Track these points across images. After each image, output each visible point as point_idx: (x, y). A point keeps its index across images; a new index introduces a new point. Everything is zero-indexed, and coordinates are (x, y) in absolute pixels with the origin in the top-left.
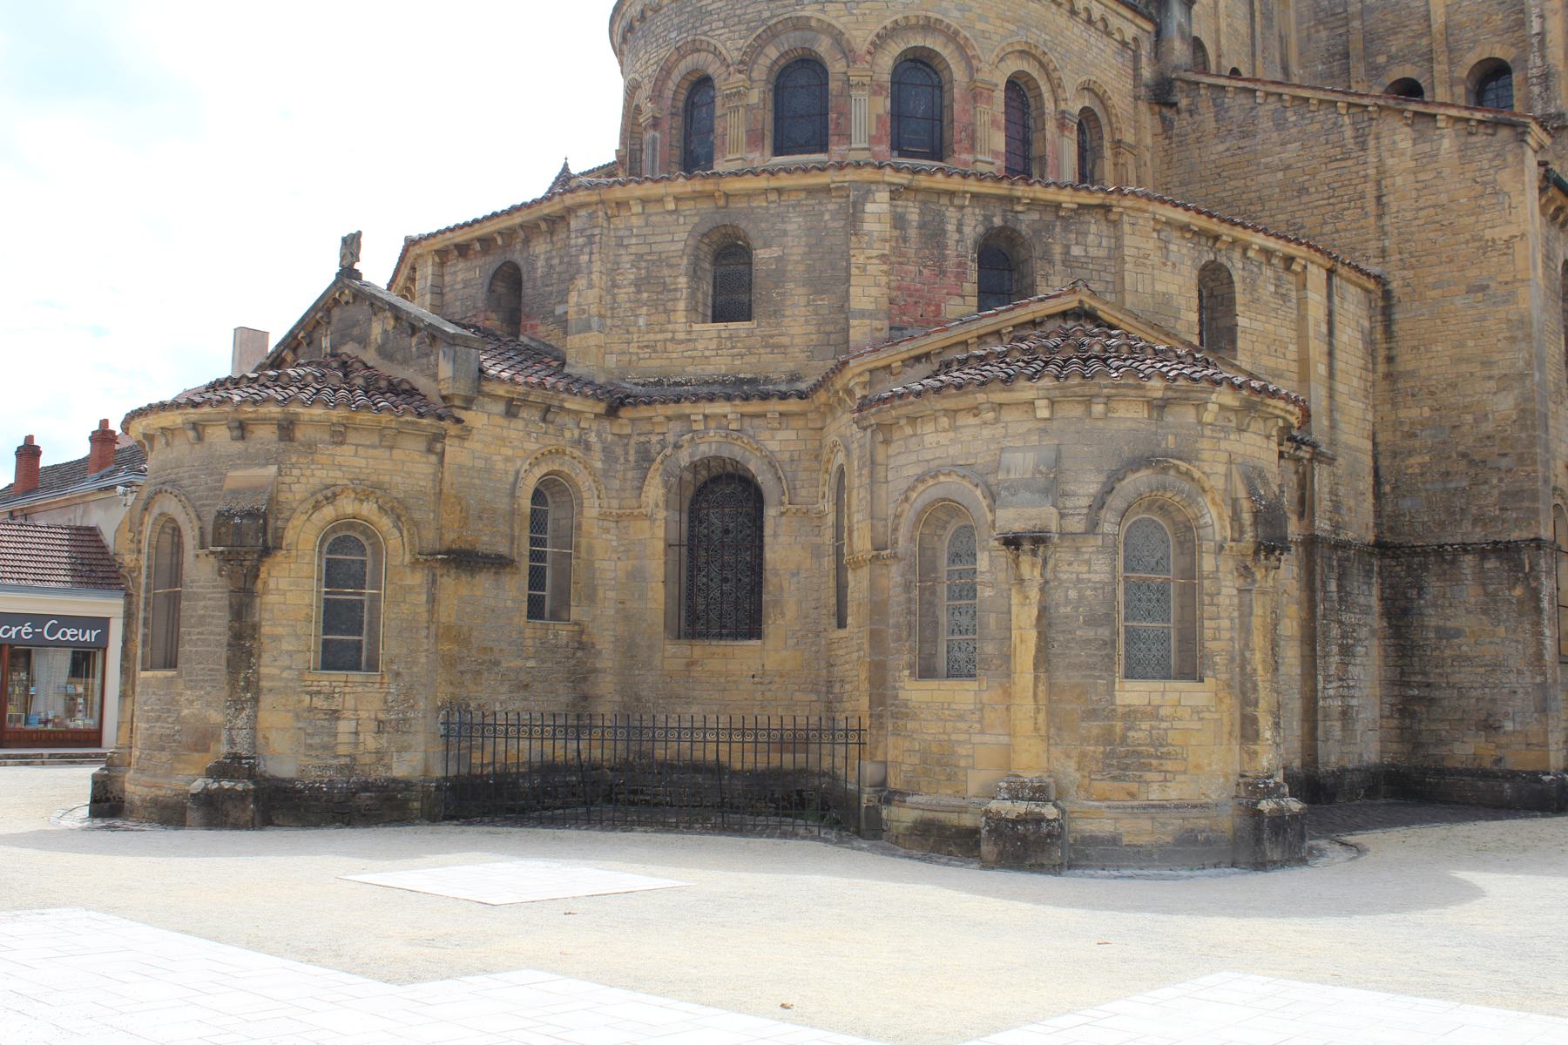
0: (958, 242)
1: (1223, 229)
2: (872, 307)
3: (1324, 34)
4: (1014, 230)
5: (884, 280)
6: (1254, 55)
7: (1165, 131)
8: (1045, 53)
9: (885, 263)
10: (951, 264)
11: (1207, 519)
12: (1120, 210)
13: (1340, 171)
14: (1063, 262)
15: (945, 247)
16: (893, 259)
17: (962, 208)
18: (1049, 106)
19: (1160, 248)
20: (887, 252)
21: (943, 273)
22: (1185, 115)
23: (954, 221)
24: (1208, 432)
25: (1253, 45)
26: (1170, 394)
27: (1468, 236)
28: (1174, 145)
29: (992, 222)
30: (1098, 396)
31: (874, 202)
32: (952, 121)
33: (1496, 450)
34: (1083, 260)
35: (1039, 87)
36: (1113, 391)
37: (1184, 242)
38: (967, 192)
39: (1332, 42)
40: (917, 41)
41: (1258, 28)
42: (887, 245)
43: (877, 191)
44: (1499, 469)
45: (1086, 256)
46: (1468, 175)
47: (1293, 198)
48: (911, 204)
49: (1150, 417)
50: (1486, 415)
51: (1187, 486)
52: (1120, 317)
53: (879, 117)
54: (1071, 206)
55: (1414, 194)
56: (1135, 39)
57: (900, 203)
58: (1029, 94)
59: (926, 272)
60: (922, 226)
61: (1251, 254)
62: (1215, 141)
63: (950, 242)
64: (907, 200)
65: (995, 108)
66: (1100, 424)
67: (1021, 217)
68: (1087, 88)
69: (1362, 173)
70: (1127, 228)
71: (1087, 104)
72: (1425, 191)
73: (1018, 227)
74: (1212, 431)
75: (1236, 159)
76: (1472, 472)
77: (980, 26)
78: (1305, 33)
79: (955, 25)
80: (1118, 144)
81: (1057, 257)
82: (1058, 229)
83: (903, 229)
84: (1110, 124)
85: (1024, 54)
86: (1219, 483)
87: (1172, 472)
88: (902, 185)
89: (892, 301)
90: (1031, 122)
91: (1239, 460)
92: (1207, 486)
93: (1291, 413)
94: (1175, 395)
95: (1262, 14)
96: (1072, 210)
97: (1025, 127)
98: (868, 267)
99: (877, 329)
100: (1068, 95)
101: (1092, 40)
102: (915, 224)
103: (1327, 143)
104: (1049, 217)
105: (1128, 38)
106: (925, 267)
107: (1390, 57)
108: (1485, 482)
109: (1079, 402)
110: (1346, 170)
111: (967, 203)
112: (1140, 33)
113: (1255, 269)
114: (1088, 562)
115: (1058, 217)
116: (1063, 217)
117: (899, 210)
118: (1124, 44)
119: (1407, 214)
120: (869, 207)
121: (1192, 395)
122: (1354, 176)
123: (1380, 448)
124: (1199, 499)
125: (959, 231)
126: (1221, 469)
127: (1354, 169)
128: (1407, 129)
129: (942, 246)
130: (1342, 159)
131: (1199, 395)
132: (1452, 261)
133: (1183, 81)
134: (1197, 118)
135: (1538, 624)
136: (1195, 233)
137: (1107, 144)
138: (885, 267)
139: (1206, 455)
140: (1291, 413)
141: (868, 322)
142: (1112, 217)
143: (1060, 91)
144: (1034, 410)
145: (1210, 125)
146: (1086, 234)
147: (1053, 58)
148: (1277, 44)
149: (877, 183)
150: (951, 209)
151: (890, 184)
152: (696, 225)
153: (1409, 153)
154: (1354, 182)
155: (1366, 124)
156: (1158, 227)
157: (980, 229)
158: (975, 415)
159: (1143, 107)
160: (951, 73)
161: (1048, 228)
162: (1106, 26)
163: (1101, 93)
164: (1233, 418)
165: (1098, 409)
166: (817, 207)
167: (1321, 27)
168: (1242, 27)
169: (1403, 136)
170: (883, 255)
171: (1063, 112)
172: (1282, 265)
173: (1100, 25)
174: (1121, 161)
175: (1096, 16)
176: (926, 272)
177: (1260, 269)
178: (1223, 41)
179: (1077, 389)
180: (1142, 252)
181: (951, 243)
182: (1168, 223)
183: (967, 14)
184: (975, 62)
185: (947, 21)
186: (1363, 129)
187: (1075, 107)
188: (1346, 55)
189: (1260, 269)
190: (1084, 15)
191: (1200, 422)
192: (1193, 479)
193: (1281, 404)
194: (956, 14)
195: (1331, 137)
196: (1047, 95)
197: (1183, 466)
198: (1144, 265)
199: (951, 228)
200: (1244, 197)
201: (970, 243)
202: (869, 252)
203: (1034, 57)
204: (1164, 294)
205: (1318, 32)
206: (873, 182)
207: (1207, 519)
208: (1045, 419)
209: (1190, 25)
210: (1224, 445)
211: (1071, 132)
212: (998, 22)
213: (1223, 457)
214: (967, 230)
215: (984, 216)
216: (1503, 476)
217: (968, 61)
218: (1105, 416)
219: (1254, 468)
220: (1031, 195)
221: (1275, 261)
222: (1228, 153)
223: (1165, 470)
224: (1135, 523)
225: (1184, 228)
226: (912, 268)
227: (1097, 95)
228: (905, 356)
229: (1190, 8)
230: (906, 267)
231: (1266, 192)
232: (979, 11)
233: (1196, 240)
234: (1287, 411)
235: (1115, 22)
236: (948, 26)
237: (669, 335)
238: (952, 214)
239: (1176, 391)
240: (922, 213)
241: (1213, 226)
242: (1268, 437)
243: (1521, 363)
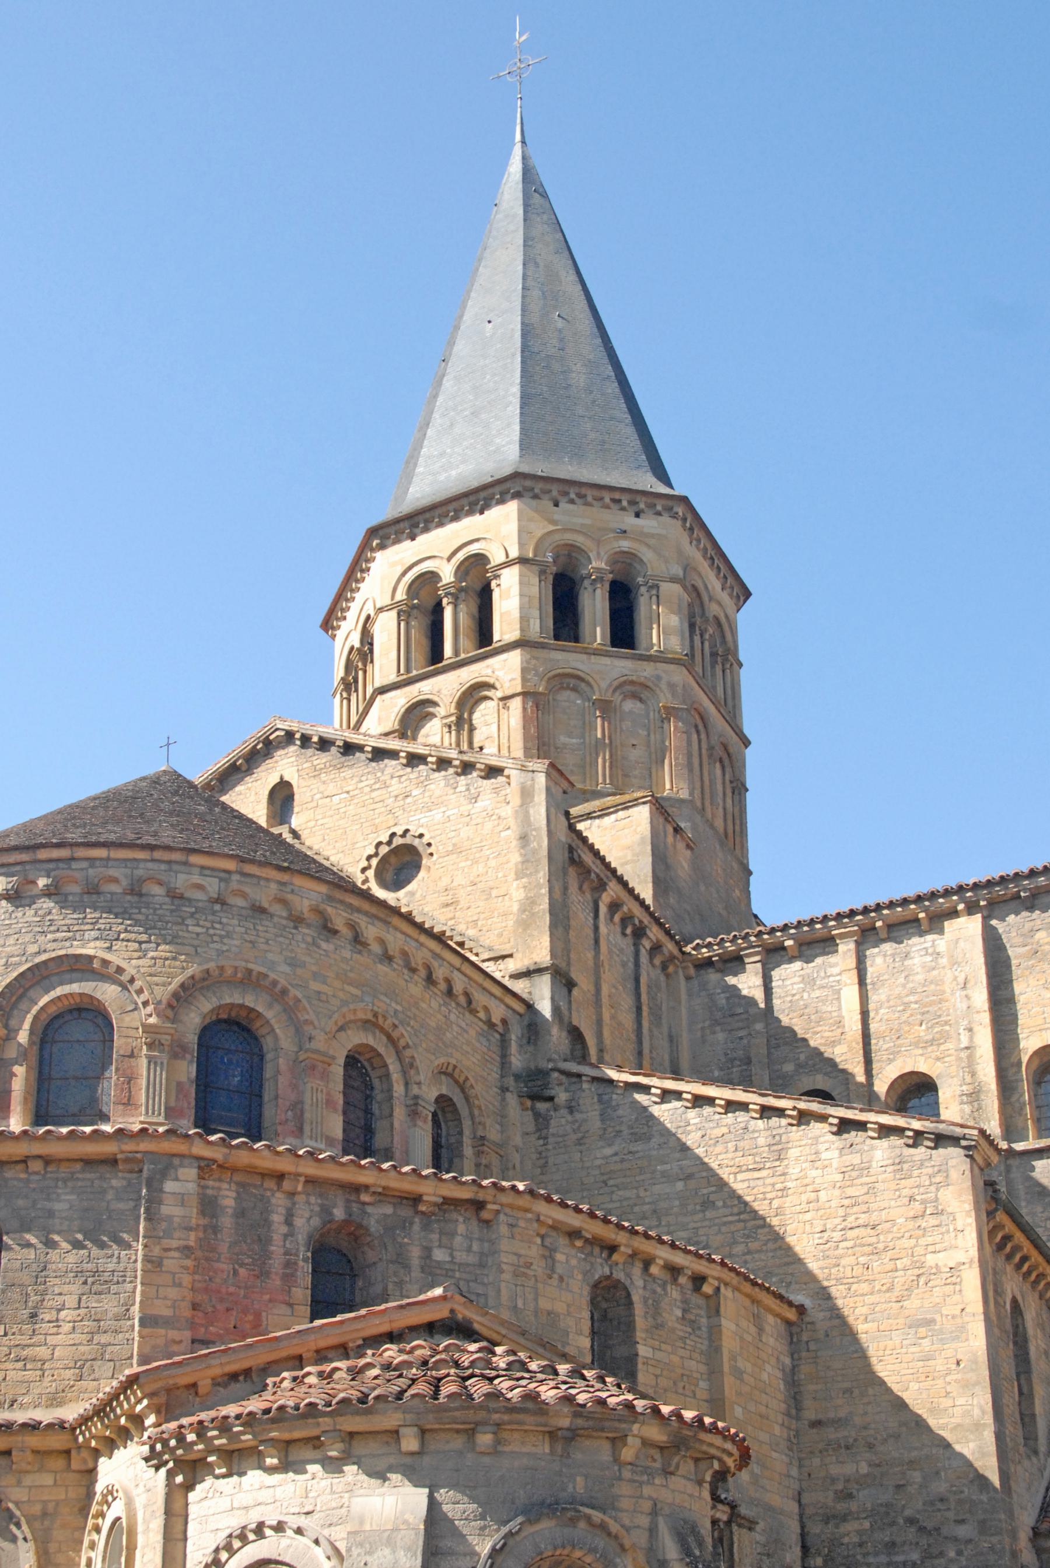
0: (286, 1236)
1: (622, 1238)
2: (167, 1312)
3: (721, 1036)
4: (360, 1226)
5: (186, 1279)
7: (538, 1130)
8: (395, 1026)
9: (188, 1257)
10: (276, 1263)
12: (496, 1207)
13: (752, 1183)
14: (422, 1268)
15: (269, 1241)
16: (199, 1253)
17: (292, 1194)
18: (399, 1089)
19: (544, 1257)
20: (192, 1244)
21: (263, 1274)
22: (564, 1112)
24: (627, 1474)
25: (640, 1042)
26: (580, 1422)
27: (906, 1261)
28: (550, 1147)
29: (331, 1214)
30: (484, 1423)
31: (177, 1179)
32: (277, 1097)
33: (951, 1515)
34: (447, 1266)
35: (385, 1066)
36: (506, 1417)
37: (573, 1252)
38: (300, 1175)
39: (731, 1046)
41: (645, 1024)
42: (193, 1235)
43: (181, 1166)
44: (956, 1539)
47: (694, 1213)
48: (225, 1186)
49: (552, 1452)
50: (937, 1473)
51: (600, 1542)
52: (504, 1332)
53: (179, 1084)
55: (841, 1212)
56: (504, 1022)
57: (211, 1183)
58: (373, 1074)
59: (242, 1271)
60: (240, 1213)
62: (601, 1143)
63: (275, 1237)
64: (220, 1180)
65: (331, 1085)
66: (486, 1460)
67: (369, 1209)
68: (446, 1072)
69: (779, 1186)
70: (504, 1230)
71: (444, 1092)
72: (855, 1209)
73: (365, 1223)
74: (633, 1472)
75: (626, 1165)
76: (924, 1542)
77: (315, 986)
78: (699, 1034)
79: (283, 982)
80: (481, 1141)
81: (415, 1262)
82: (416, 1227)
83: (214, 1216)
84: (472, 1116)
85: (371, 1024)
86: (641, 1538)
87: (582, 1524)
88: (214, 1161)
89: (195, 1307)
90: (375, 1108)
91: (667, 1510)
92: (627, 1543)
93: (730, 1454)
94: (586, 1424)
95: (650, 1008)
96: (435, 1204)
97: (368, 1111)
98: (166, 1262)
99: (174, 1342)
100: (422, 1078)
101: (453, 1017)
102: (230, 1211)
103: (736, 1150)
104: (406, 1212)
105: (496, 1019)
106: (242, 1265)
107: (799, 1066)
108: (941, 1554)
109: (458, 1431)
110: (760, 1182)
111: (300, 1188)
112: (509, 1014)
113: (659, 1290)
115: (417, 1212)
116: (423, 1213)
117: (209, 1192)
118: (491, 1025)
119: (835, 1234)
120: (169, 1186)
121: (607, 1424)
122: (769, 1189)
124: (618, 1560)
125: (289, 1221)
126: (644, 1521)
127: (769, 1181)
129: (264, 1241)
130: (754, 1170)
131: (617, 1424)
132: (888, 1290)
133: (563, 1072)
134: (578, 1116)
136: (587, 1240)
137: (467, 1140)
138: (189, 1263)
139: (625, 1503)
140: (730, 1454)
141: (162, 1331)
142: (485, 1215)
143: (412, 1072)
144: (398, 1440)
145: (595, 1124)
146: (453, 1234)
147: (406, 1036)
148: (665, 1044)
149: (182, 1156)
150: (278, 1195)
151: (199, 1158)
153: (835, 1164)
154: (769, 1196)
155: (782, 1131)
156: (543, 1231)
157: (316, 1222)
158: (315, 1448)
160: (276, 1038)
161: (405, 1225)
162: (470, 1002)
163: (461, 1080)
164: (658, 1456)
165: (485, 1439)
166: (97, 1183)
167: (718, 1028)
168: (627, 1019)
169: (827, 1145)
170: (188, 1247)
171: (416, 1097)
172: (690, 1285)
173: (462, 1000)
174: (484, 1162)
175: (458, 987)
176: (242, 1271)
177: (664, 1289)
178: (606, 1033)
179: (457, 1414)
180: (522, 1260)
181: (277, 1238)
182: (555, 1227)
183: (299, 971)
184: (308, 1029)
185: (272, 976)
186: (780, 1135)
187: (430, 1093)
188: (748, 1061)
189: (664, 1289)
190: (443, 986)
191: (616, 1460)
192: (609, 1534)
193: (717, 1440)
194: (287, 969)
195: (741, 1144)
196: (396, 1076)
197: (597, 1516)
198: (525, 1275)
199: (277, 1218)
200: (636, 1209)
201: (301, 1238)
202: (166, 1243)
203: (382, 1030)
204: (549, 1313)
205: (714, 1033)
208: (412, 1454)
209: (570, 1009)
210: (647, 1491)
211: (425, 1122)
212: (337, 984)
213: (647, 1506)
214: (299, 1222)
215: (322, 1206)
216: (963, 1547)
217: (298, 1029)
218: (495, 1451)
219: (685, 1522)
220: (384, 1183)
221: (682, 1280)
222: (615, 1158)
223: (573, 1522)
225: (574, 1234)
226: (225, 1266)
227: (457, 1082)
228: (217, 1371)
229: (570, 991)
230: (216, 1265)
231: (663, 1205)
232: (314, 968)
233: (588, 1248)
234: (724, 1451)
235: (479, 998)
236: (275, 983)
238: (279, 1200)
239: (588, 1418)
240: (238, 1198)
241: (609, 1234)
242: (700, 1483)
243: (977, 1412)
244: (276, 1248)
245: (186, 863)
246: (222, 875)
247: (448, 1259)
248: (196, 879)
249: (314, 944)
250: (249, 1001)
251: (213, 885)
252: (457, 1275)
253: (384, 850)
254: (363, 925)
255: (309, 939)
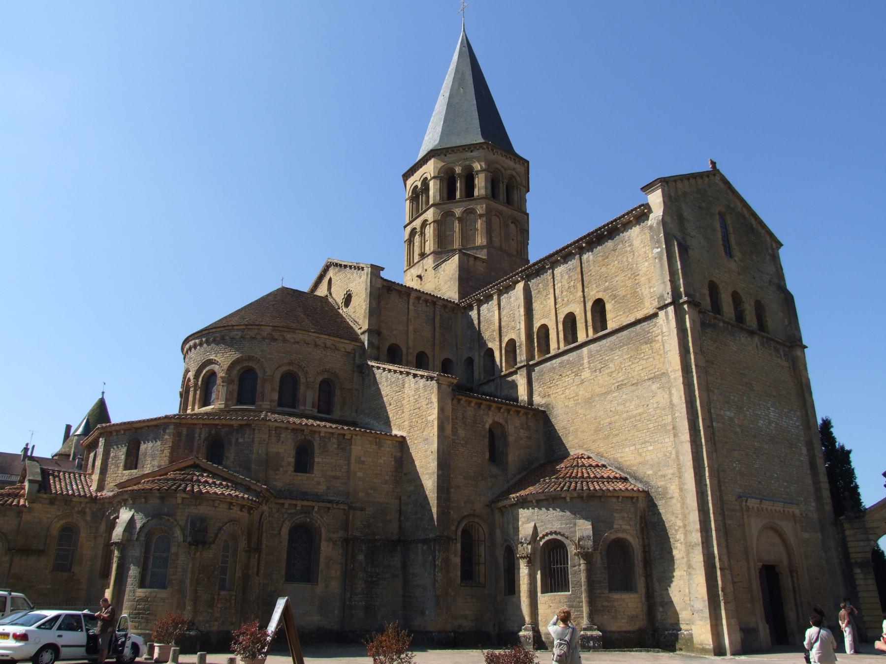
0: (198, 440)
6: (434, 345)
11: (176, 535)
12: (254, 425)
23: (198, 433)
31: (169, 429)
40: (246, 364)
45: (244, 442)
46: (426, 396)
54: (236, 425)
61: (321, 435)
72: (416, 403)
86: (182, 523)
102: (184, 435)
114: (135, 549)
117: (180, 431)
123: (402, 502)
127: (401, 395)
128: (413, 379)
135: (434, 571)
152: (129, 438)
159: (356, 374)
180: (262, 439)
181: (196, 441)
185: (256, 356)
206: (168, 423)
207: (176, 535)
214: (203, 436)
224: (159, 537)
237: (117, 475)
244: (196, 444)
245: (233, 329)
246: (242, 330)
247: (243, 441)
248: (236, 333)
249: (270, 344)
250: (250, 364)
251: (240, 333)
252: (245, 445)
253: (346, 296)
254: (285, 335)
255: (268, 343)
